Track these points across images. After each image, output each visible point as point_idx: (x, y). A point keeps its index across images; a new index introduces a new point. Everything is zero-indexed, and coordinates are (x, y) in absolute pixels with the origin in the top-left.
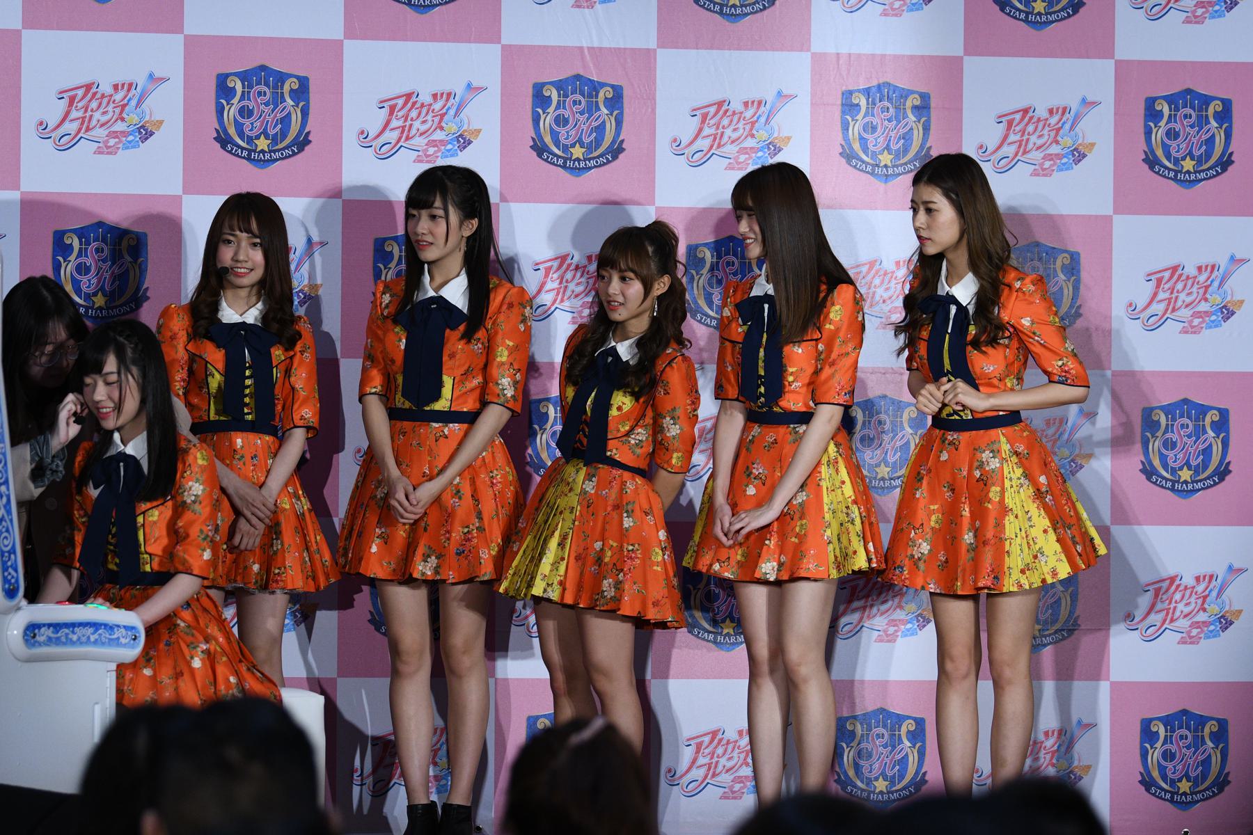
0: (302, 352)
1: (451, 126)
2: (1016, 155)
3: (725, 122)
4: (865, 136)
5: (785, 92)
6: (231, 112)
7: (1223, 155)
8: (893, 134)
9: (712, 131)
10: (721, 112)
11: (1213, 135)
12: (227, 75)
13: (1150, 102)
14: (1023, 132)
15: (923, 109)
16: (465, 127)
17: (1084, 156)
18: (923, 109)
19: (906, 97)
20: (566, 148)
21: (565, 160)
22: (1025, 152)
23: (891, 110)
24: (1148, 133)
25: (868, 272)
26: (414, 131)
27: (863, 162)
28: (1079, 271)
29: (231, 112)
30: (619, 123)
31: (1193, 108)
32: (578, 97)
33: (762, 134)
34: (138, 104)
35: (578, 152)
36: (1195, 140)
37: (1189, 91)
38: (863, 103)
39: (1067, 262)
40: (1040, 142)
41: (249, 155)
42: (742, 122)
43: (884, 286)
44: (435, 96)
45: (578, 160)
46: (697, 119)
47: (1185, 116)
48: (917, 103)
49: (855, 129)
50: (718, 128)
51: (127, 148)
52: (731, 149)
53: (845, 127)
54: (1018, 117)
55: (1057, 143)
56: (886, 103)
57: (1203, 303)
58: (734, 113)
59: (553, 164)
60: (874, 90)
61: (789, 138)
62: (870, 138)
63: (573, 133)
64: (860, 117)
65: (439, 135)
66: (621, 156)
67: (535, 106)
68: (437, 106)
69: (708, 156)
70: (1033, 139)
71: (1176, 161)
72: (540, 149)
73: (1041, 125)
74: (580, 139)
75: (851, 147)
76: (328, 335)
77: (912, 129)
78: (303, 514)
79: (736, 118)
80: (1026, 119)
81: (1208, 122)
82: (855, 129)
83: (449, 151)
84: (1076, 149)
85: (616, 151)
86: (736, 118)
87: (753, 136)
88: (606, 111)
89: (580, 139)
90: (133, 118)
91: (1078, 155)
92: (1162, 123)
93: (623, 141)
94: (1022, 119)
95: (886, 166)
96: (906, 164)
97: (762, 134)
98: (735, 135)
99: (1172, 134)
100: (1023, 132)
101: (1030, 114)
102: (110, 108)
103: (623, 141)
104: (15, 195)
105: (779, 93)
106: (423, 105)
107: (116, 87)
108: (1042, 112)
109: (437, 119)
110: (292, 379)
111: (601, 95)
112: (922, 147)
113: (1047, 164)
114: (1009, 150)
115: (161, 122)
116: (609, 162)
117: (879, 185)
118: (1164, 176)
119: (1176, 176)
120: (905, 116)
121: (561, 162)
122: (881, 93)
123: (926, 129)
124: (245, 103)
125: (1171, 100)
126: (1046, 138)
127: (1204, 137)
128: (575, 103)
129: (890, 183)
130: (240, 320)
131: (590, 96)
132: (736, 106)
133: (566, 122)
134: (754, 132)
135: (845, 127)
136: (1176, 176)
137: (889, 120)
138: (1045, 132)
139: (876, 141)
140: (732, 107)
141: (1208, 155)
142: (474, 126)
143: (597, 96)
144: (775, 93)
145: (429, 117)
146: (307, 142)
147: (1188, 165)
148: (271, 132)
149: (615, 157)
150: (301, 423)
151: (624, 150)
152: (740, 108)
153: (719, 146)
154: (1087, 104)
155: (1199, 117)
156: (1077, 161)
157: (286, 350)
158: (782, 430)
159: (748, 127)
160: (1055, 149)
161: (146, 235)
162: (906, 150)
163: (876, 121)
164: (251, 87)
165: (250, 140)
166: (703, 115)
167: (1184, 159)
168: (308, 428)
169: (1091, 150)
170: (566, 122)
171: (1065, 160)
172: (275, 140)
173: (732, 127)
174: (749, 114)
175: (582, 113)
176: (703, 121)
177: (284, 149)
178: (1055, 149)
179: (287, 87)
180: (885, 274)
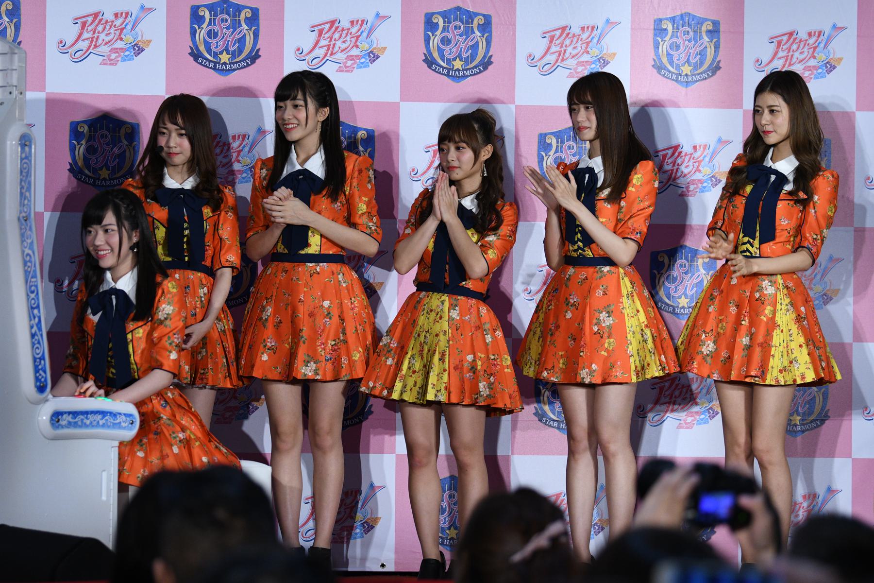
0: (227, 212)
1: (364, 45)
3: (567, 42)
4: (671, 52)
5: (612, 20)
6: (202, 34)
8: (692, 51)
9: (558, 49)
10: (564, 35)
12: (199, 7)
15: (714, 32)
16: (375, 46)
17: (835, 67)
19: (702, 24)
20: (449, 62)
21: (449, 70)
26: (336, 49)
27: (670, 72)
28: (830, 154)
29: (202, 34)
30: (489, 42)
33: (594, 52)
34: (133, 28)
35: (458, 64)
40: (801, 57)
41: (215, 66)
42: (580, 42)
44: (352, 22)
45: (458, 70)
46: (547, 40)
48: (710, 28)
49: (664, 47)
50: (562, 47)
51: (124, 60)
52: (571, 63)
53: (656, 46)
54: (785, 38)
55: (814, 57)
58: (574, 35)
59: (440, 73)
60: (678, 18)
61: (615, 54)
62: (675, 54)
63: (454, 50)
64: (667, 38)
65: (355, 52)
66: (490, 67)
67: (426, 30)
68: (354, 30)
69: (554, 67)
70: (797, 55)
72: (430, 62)
73: (802, 44)
75: (660, 61)
76: (245, 199)
77: (706, 47)
78: (224, 331)
79: (575, 39)
82: (664, 47)
83: (362, 63)
85: (486, 64)
86: (575, 39)
87: (588, 53)
88: (479, 34)
90: (129, 38)
93: (491, 56)
94: (788, 41)
95: (686, 75)
96: (701, 73)
97: (594, 52)
98: (574, 52)
101: (794, 36)
102: (112, 31)
103: (491, 56)
104: (42, 95)
105: (608, 21)
106: (343, 29)
107: (116, 15)
108: (803, 35)
109: (353, 40)
110: (220, 232)
111: (475, 22)
115: (150, 41)
116: (481, 72)
117: (681, 90)
120: (701, 38)
121: (445, 72)
122: (683, 20)
123: (717, 47)
124: (212, 27)
126: (806, 54)
128: (456, 27)
130: (180, 187)
131: (467, 22)
132: (576, 30)
133: (449, 42)
134: (589, 49)
135: (656, 46)
137: (689, 41)
138: (805, 50)
139: (679, 56)
140: (573, 31)
142: (381, 45)
143: (472, 23)
144: (605, 20)
145: (348, 39)
146: (257, 56)
148: (231, 49)
149: (485, 68)
150: (227, 264)
151: (492, 63)
152: (578, 31)
153: (563, 60)
156: (829, 72)
157: (213, 211)
158: (591, 270)
159: (584, 46)
160: (812, 63)
161: (138, 125)
162: (701, 63)
163: (679, 41)
164: (216, 15)
165: (215, 55)
168: (233, 268)
170: (449, 42)
171: (820, 71)
172: (234, 55)
173: (572, 46)
174: (585, 36)
175: (461, 35)
176: (551, 42)
177: (240, 61)
178: (812, 63)
179: (242, 16)
180: (686, 155)
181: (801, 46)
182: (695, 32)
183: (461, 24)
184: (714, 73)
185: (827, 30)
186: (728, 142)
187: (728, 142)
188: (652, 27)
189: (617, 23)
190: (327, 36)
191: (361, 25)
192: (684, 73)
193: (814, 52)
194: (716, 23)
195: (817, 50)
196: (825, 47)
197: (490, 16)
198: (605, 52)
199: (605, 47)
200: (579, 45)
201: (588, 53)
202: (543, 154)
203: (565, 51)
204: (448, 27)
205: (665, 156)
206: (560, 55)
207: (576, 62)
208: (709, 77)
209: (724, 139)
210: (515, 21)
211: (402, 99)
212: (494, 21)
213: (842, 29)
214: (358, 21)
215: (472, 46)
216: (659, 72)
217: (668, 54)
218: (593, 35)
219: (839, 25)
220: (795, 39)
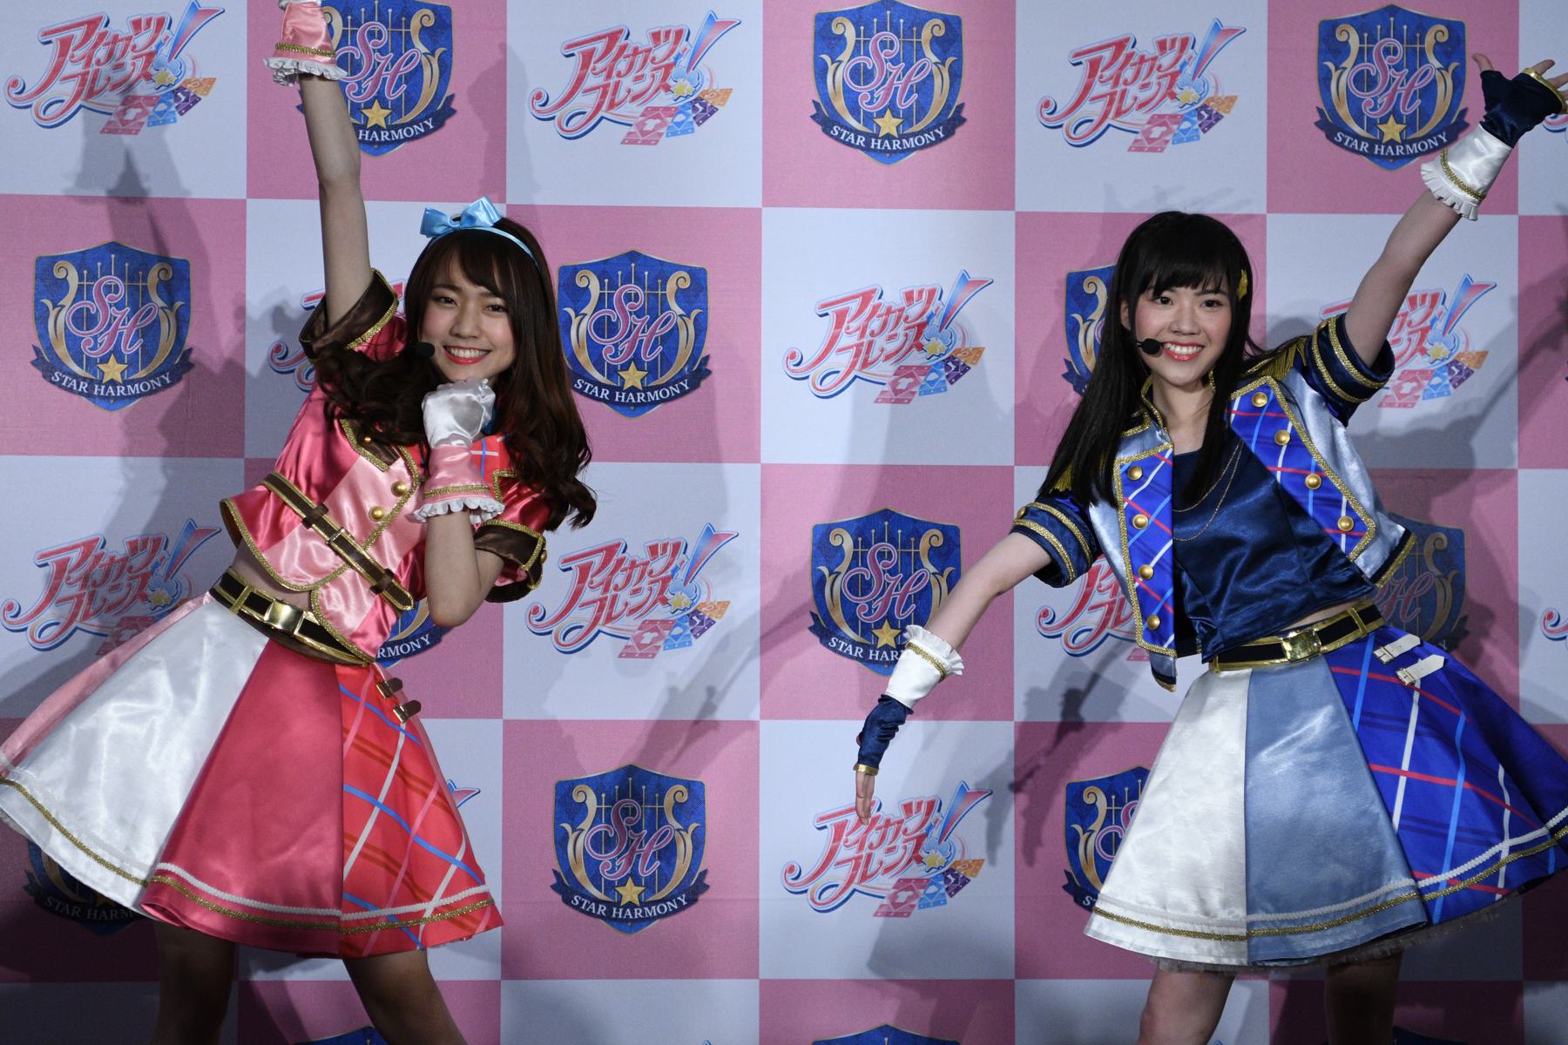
2: (1105, 116)
3: (622, 65)
5: (721, 17)
7: (1449, 115)
8: (899, 84)
9: (600, 80)
11: (1434, 82)
13: (1328, 30)
17: (1218, 118)
18: (949, 42)
19: (921, 27)
24: (1324, 79)
25: (860, 311)
27: (851, 129)
32: (377, 25)
33: (683, 86)
36: (1402, 90)
44: (137, 24)
46: (573, 65)
47: (1387, 51)
48: (940, 33)
49: (839, 74)
50: (609, 76)
52: (632, 110)
53: (821, 72)
54: (1107, 55)
56: (889, 35)
57: (1418, 356)
58: (636, 51)
61: (728, 92)
68: (141, 40)
69: (593, 121)
70: (1133, 90)
71: (1372, 125)
74: (381, 93)
75: (829, 105)
77: (931, 76)
79: (639, 59)
80: (1122, 58)
81: (1424, 60)
82: (839, 74)
84: (1204, 107)
85: (440, 114)
87: (668, 89)
89: (381, 93)
91: (1208, 116)
92: (1348, 63)
96: (921, 132)
97: (683, 86)
98: (638, 88)
99: (1364, 81)
101: (1128, 49)
111: (415, 23)
112: (948, 107)
113: (1157, 132)
114: (1092, 109)
116: (428, 132)
118: (1353, 150)
119: (1371, 148)
120: (921, 54)
123: (955, 75)
125: (1362, 24)
126: (1154, 88)
127: (1418, 85)
128: (371, 35)
131: (397, 24)
134: (670, 82)
135: (821, 72)
136: (1371, 148)
138: (1153, 79)
141: (1425, 114)
142: (204, 73)
143: (408, 26)
144: (703, 17)
147: (1392, 130)
149: (439, 124)
151: (454, 111)
153: (612, 105)
154: (1222, 32)
155: (1410, 53)
156: (1206, 127)
162: (922, 109)
163: (870, 62)
166: (584, 54)
167: (1384, 121)
169: (1229, 107)
171: (1185, 125)
173: (633, 74)
175: (383, 52)
176: (585, 65)
178: (1169, 107)
181: (1144, 73)
182: (907, 45)
183: (382, 27)
184: (949, 133)
185: (1201, 35)
186: (982, 284)
187: (982, 284)
190: (78, 53)
191: (158, 30)
193: (1171, 85)
194: (953, 24)
197: (448, 10)
198: (706, 86)
199: (707, 76)
200: (647, 71)
201: (668, 89)
204: (354, 33)
206: (604, 96)
207: (642, 109)
208: (939, 140)
209: (974, 276)
210: (505, 21)
211: (252, 193)
212: (457, 20)
213: (1234, 32)
214: (149, 22)
216: (827, 129)
217: (846, 90)
218: (679, 49)
219: (1227, 24)
220: (1130, 56)
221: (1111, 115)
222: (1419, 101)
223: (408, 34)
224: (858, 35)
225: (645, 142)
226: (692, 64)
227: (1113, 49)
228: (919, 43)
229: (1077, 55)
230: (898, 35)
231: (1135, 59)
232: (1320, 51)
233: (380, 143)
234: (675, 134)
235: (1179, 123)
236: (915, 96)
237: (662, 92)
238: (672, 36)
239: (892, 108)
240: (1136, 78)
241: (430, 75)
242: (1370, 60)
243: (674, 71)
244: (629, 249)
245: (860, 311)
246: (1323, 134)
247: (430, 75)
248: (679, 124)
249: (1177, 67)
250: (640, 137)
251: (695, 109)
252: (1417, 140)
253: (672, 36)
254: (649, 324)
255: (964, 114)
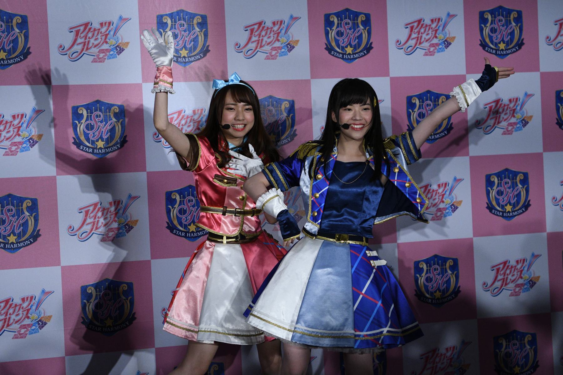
2: (256, 48)
3: (90, 35)
5: (124, 17)
8: (187, 39)
9: (83, 40)
10: (87, 30)
11: (361, 34)
14: (259, 35)
15: (203, 24)
17: (294, 47)
18: (203, 24)
22: (261, 47)
23: (185, 25)
24: (327, 33)
30: (26, 37)
31: (350, 19)
33: (112, 41)
37: (347, 10)
38: (169, 22)
39: (288, 106)
40: (269, 40)
42: (100, 35)
43: (187, 125)
46: (73, 35)
48: (200, 21)
50: (86, 39)
52: (95, 50)
54: (256, 27)
55: (278, 40)
56: (182, 22)
58: (95, 30)
61: (128, 43)
69: (81, 55)
70: (265, 39)
71: (343, 49)
77: (197, 36)
80: (261, 28)
81: (358, 27)
84: (289, 44)
85: (26, 54)
86: (96, 33)
87: (107, 43)
88: (18, 31)
95: (184, 57)
96: (195, 55)
97: (112, 41)
99: (340, 34)
100: (259, 35)
101: (263, 25)
103: (29, 48)
105: (121, 17)
108: (269, 24)
112: (204, 46)
113: (274, 53)
114: (252, 46)
118: (337, 57)
119: (343, 56)
120: (194, 29)
123: (206, 35)
125: (338, 15)
126: (272, 38)
127: (357, 35)
129: (187, 67)
132: (96, 25)
134: (107, 40)
136: (343, 56)
137: (185, 31)
138: (272, 35)
141: (359, 44)
143: (12, 22)
144: (118, 17)
151: (30, 53)
152: (98, 26)
153: (87, 49)
154: (294, 19)
155: (354, 24)
159: (103, 38)
160: (277, 44)
162: (195, 48)
167: (347, 47)
169: (297, 44)
171: (283, 50)
173: (94, 38)
174: (103, 30)
178: (277, 44)
184: (205, 55)
185: (286, 19)
188: (155, 21)
189: (127, 20)
192: (182, 56)
194: (204, 18)
195: (280, 35)
196: (286, 32)
197: (26, 17)
198: (120, 41)
199: (120, 38)
200: (99, 37)
201: (107, 43)
202: (77, 122)
203: (89, 42)
205: (172, 118)
207: (98, 50)
208: (201, 58)
212: (30, 20)
213: (297, 19)
215: (13, 41)
218: (110, 29)
219: (295, 16)
220: (264, 27)
221: (259, 47)
222: (357, 40)
223: (12, 26)
224: (172, 22)
225: (100, 62)
226: (115, 34)
227: (258, 25)
228: (193, 24)
229: (246, 27)
230: (185, 22)
231: (265, 28)
232: (325, 24)
233: (4, 65)
234: (110, 58)
235: (281, 50)
236: (193, 43)
237: (105, 44)
238: (107, 24)
239: (185, 47)
240: (266, 34)
241: (21, 40)
242: (341, 27)
243: (109, 36)
244: (97, 99)
245: (178, 117)
246: (327, 52)
247: (21, 40)
248: (111, 55)
249: (279, 31)
250: (98, 60)
251: (117, 50)
252: (357, 53)
253: (107, 24)
254: (105, 125)
255: (209, 49)
